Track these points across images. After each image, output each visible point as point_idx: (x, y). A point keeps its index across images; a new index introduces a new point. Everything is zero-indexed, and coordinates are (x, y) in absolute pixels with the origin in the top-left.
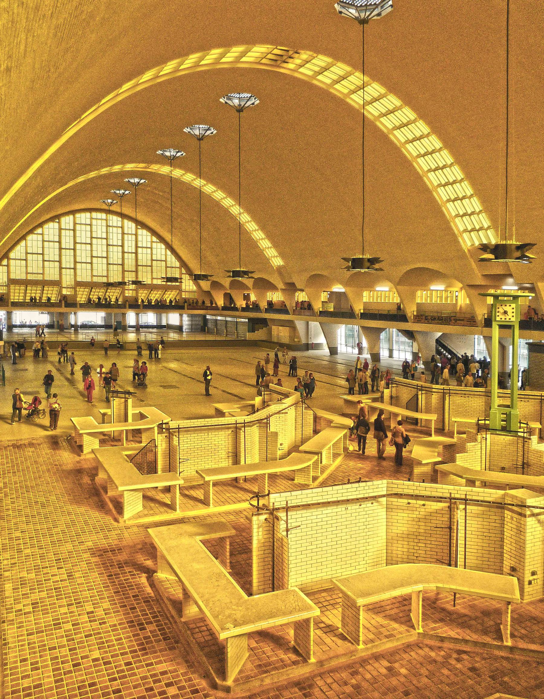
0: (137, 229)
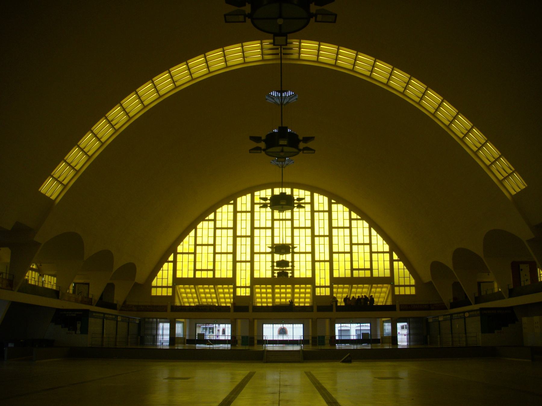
0: (330, 204)
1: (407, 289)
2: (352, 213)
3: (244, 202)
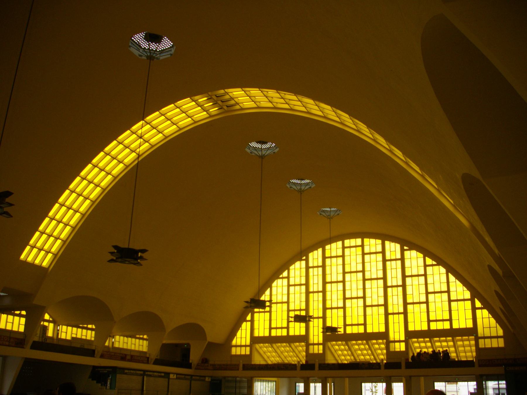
0: (402, 251)
1: (494, 341)
2: (427, 258)
3: (315, 257)
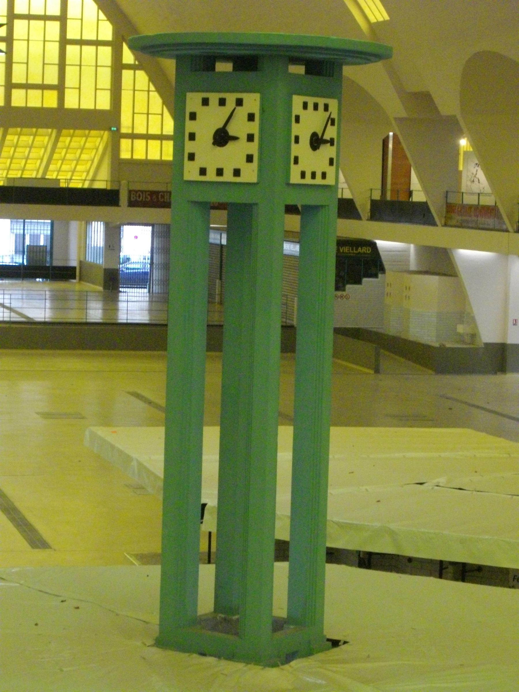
1: (154, 145)
